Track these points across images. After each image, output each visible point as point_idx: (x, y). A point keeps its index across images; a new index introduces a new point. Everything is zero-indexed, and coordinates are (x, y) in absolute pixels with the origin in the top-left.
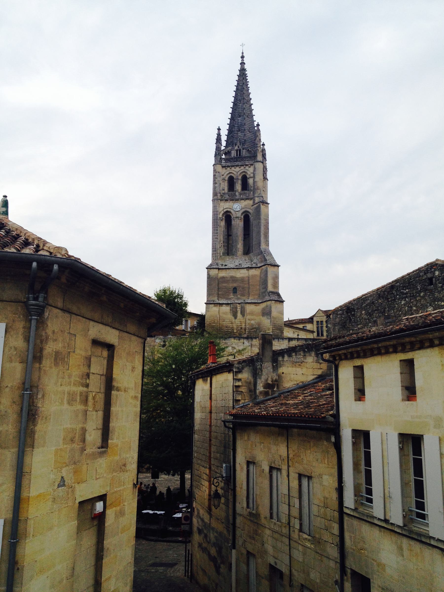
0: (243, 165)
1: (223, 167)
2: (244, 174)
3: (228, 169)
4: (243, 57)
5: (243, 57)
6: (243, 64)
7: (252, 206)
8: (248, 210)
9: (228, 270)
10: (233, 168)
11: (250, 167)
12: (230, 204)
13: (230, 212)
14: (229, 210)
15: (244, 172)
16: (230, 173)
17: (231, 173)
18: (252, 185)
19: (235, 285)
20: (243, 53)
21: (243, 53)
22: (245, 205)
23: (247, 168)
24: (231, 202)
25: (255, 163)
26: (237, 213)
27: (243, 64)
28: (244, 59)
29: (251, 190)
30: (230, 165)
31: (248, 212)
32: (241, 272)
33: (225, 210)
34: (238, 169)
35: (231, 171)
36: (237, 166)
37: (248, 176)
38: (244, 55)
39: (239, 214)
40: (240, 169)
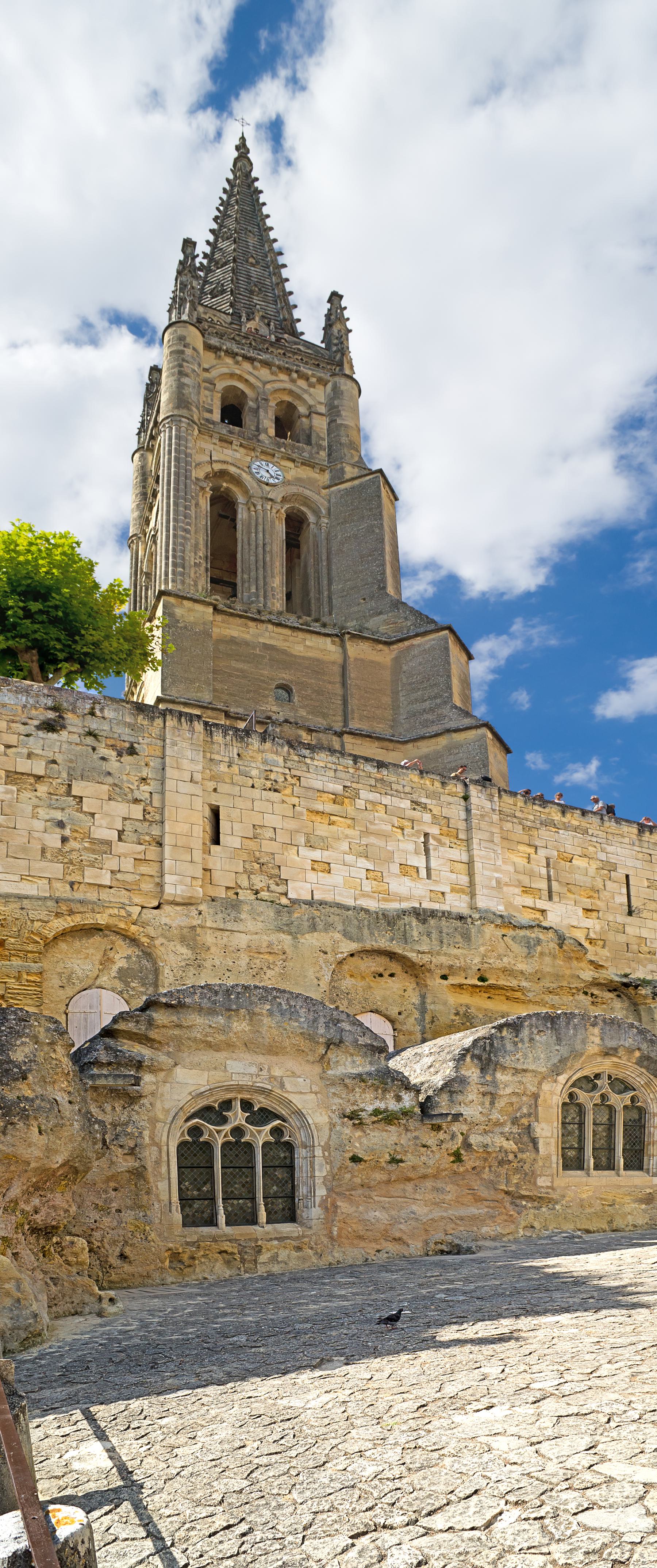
1: (208, 347)
2: (287, 398)
3: (229, 360)
7: (325, 488)
8: (307, 493)
9: (251, 624)
10: (247, 366)
12: (238, 455)
13: (237, 481)
14: (232, 470)
15: (291, 392)
16: (232, 375)
17: (240, 378)
18: (324, 434)
22: (299, 480)
23: (302, 383)
24: (242, 450)
26: (268, 488)
29: (320, 447)
30: (236, 350)
31: (306, 501)
32: (308, 643)
33: (217, 467)
34: (264, 373)
35: (238, 372)
36: (266, 364)
37: (302, 410)
39: (277, 494)
40: (274, 378)
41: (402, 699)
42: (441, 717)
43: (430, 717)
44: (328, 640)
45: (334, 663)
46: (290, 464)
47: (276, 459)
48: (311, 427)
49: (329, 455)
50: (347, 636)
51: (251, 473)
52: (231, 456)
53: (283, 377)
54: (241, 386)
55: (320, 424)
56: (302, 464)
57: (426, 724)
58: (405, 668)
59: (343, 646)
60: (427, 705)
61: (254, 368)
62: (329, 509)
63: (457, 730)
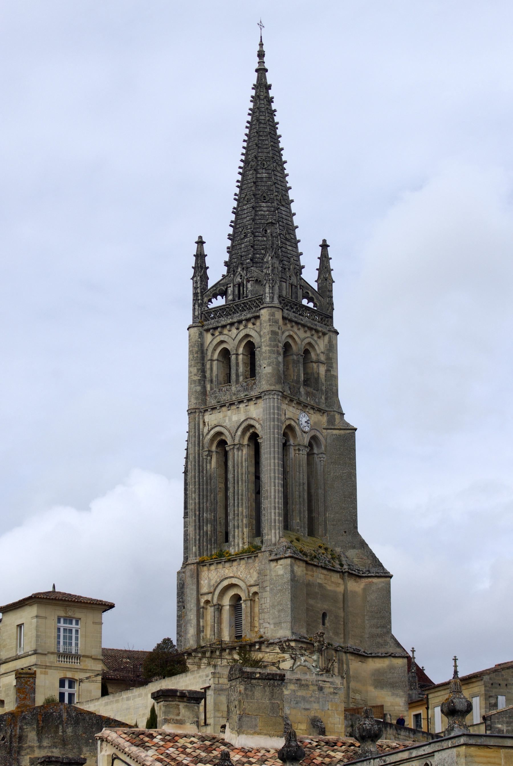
0: (311, 329)
4: (261, 55)
5: (261, 55)
6: (262, 71)
7: (324, 429)
10: (295, 329)
11: (319, 337)
19: (325, 606)
20: (261, 45)
21: (261, 45)
25: (331, 334)
27: (262, 71)
28: (265, 59)
32: (333, 579)
37: (313, 356)
38: (265, 48)
41: (367, 622)
42: (386, 643)
43: (380, 640)
44: (338, 575)
45: (340, 592)
46: (312, 411)
47: (307, 410)
48: (318, 374)
49: (326, 399)
50: (346, 574)
51: (299, 425)
52: (291, 411)
53: (308, 334)
54: (290, 341)
55: (322, 370)
56: (318, 410)
57: (379, 645)
58: (368, 599)
59: (343, 579)
60: (379, 631)
61: (299, 329)
62: (326, 447)
63: (392, 656)
